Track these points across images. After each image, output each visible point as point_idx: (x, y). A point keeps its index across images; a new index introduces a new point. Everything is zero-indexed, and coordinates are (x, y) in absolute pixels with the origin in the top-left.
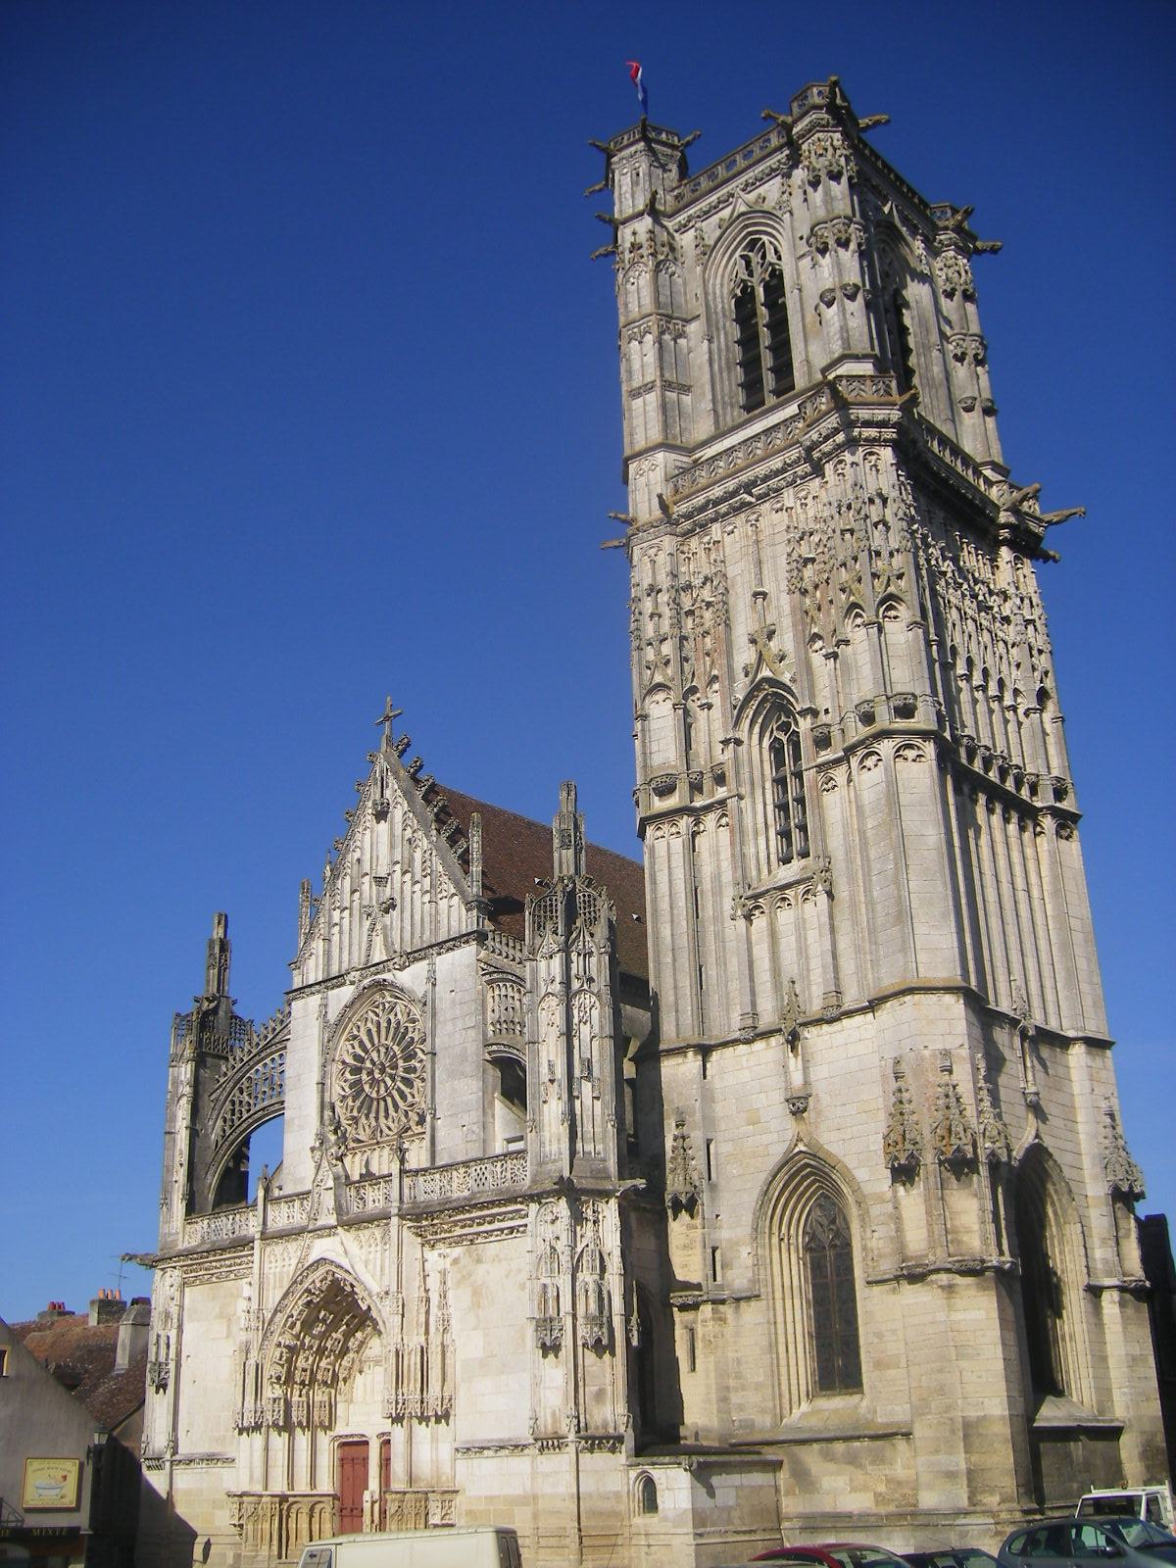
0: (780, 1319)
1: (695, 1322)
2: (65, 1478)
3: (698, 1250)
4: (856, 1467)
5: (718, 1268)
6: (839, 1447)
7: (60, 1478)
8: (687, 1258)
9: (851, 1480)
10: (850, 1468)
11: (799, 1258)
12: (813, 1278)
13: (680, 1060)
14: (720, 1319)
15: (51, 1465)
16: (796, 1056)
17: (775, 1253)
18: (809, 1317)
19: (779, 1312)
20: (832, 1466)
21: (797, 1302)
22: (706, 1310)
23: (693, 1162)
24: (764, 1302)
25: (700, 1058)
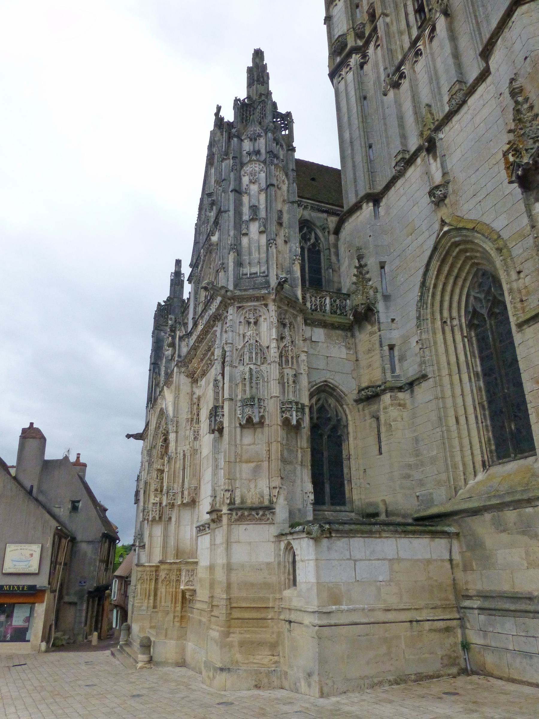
0: (448, 393)
1: (378, 411)
2: (32, 555)
3: (377, 351)
4: (531, 538)
5: (397, 362)
6: (511, 515)
7: (28, 555)
8: (370, 360)
9: (527, 553)
10: (525, 538)
11: (463, 337)
12: (481, 351)
13: (358, 213)
14: (400, 405)
15: (23, 548)
16: (435, 160)
17: (440, 336)
18: (480, 389)
19: (447, 387)
20: (505, 537)
21: (465, 377)
22: (386, 398)
23: (370, 283)
24: (431, 380)
25: (371, 204)
